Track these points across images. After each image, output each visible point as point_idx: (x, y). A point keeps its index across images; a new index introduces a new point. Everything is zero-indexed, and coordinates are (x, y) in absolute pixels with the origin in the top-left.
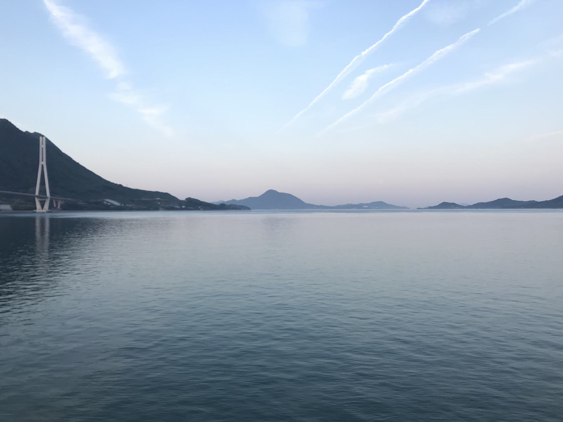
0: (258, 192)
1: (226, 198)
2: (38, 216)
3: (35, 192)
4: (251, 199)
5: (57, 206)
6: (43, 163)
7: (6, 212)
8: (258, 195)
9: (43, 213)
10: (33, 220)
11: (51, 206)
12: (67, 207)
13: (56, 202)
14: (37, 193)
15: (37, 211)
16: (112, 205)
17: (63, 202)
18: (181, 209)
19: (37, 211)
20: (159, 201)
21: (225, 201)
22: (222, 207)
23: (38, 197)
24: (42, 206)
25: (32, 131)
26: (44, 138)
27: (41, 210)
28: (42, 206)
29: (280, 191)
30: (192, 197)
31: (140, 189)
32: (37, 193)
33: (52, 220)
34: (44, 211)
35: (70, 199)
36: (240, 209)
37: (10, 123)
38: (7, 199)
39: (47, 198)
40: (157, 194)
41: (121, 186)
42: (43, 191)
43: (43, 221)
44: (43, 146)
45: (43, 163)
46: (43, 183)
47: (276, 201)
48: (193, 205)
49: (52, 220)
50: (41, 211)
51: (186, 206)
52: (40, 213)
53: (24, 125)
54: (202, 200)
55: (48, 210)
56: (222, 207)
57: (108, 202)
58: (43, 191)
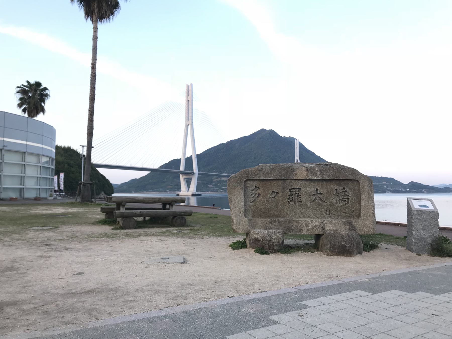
20: (385, 185)
25: (287, 136)
30: (415, 181)
37: (275, 132)
44: (297, 146)
53: (283, 133)
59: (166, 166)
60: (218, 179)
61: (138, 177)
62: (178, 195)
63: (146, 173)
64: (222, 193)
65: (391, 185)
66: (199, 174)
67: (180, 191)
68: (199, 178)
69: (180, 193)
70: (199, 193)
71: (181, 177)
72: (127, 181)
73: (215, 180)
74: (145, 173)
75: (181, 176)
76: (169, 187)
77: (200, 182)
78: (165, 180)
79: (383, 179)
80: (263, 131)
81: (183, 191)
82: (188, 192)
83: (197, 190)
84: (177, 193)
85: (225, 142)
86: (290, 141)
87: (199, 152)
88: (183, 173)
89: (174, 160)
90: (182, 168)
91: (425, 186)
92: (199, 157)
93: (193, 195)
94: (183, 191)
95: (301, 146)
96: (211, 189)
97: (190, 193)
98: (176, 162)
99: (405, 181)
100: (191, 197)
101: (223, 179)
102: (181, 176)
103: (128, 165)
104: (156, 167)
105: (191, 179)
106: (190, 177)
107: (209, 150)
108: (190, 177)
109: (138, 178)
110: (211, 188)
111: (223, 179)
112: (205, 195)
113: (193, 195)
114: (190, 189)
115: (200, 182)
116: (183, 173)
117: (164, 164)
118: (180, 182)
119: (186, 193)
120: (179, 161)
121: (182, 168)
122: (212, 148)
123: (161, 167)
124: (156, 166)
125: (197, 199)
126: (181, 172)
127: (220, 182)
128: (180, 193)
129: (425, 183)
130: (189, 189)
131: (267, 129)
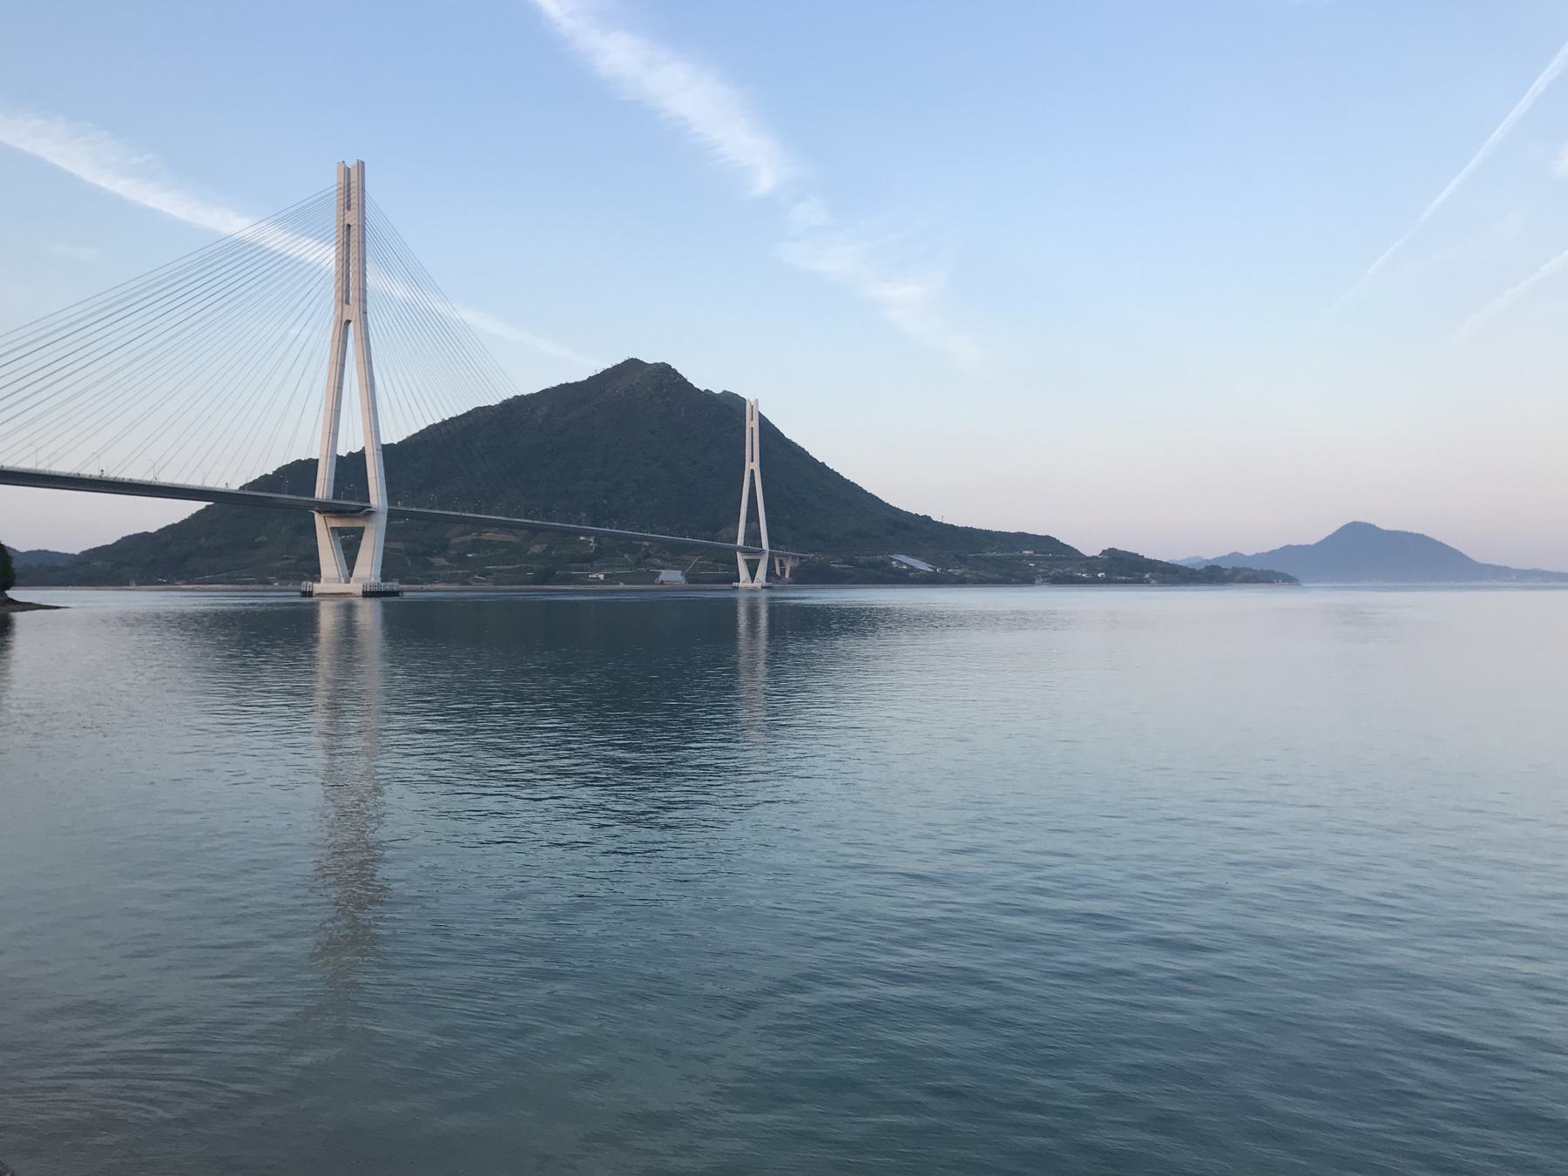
0: (1313, 529)
4: (1289, 551)
5: (783, 572)
6: (753, 465)
9: (754, 590)
10: (732, 605)
11: (770, 574)
13: (781, 564)
14: (740, 542)
15: (740, 585)
16: (912, 569)
17: (797, 563)
19: (740, 585)
21: (1249, 553)
25: (717, 391)
27: (750, 582)
29: (1386, 525)
31: (976, 527)
32: (740, 542)
37: (675, 372)
38: (675, 556)
39: (762, 552)
41: (927, 519)
42: (753, 536)
44: (752, 425)
45: (753, 465)
47: (1370, 554)
48: (1124, 568)
49: (772, 610)
53: (705, 376)
55: (765, 583)
57: (901, 563)
58: (753, 536)
59: (264, 482)
60: (468, 538)
62: (309, 594)
64: (486, 586)
66: (391, 515)
68: (391, 534)
69: (318, 588)
70: (394, 585)
75: (319, 520)
76: (278, 564)
77: (399, 545)
78: (263, 538)
79: (1022, 539)
80: (633, 365)
81: (327, 580)
82: (348, 582)
83: (385, 577)
84: (306, 585)
85: (495, 401)
87: (395, 432)
89: (299, 461)
90: (323, 488)
91: (1151, 561)
92: (391, 454)
93: (366, 594)
94: (327, 580)
95: (764, 423)
96: (442, 573)
97: (355, 587)
98: (302, 472)
100: (360, 602)
101: (489, 535)
102: (319, 520)
103: (91, 471)
105: (359, 533)
106: (358, 523)
107: (432, 429)
108: (358, 523)
109: (152, 530)
110: (443, 567)
111: (489, 535)
112: (411, 593)
113: (366, 594)
115: (399, 545)
116: (327, 509)
118: (316, 547)
119: (341, 587)
120: (312, 465)
121: (323, 488)
122: (444, 423)
125: (385, 606)
126: (319, 503)
127: (476, 546)
128: (318, 588)
129: (1149, 554)
131: (649, 359)
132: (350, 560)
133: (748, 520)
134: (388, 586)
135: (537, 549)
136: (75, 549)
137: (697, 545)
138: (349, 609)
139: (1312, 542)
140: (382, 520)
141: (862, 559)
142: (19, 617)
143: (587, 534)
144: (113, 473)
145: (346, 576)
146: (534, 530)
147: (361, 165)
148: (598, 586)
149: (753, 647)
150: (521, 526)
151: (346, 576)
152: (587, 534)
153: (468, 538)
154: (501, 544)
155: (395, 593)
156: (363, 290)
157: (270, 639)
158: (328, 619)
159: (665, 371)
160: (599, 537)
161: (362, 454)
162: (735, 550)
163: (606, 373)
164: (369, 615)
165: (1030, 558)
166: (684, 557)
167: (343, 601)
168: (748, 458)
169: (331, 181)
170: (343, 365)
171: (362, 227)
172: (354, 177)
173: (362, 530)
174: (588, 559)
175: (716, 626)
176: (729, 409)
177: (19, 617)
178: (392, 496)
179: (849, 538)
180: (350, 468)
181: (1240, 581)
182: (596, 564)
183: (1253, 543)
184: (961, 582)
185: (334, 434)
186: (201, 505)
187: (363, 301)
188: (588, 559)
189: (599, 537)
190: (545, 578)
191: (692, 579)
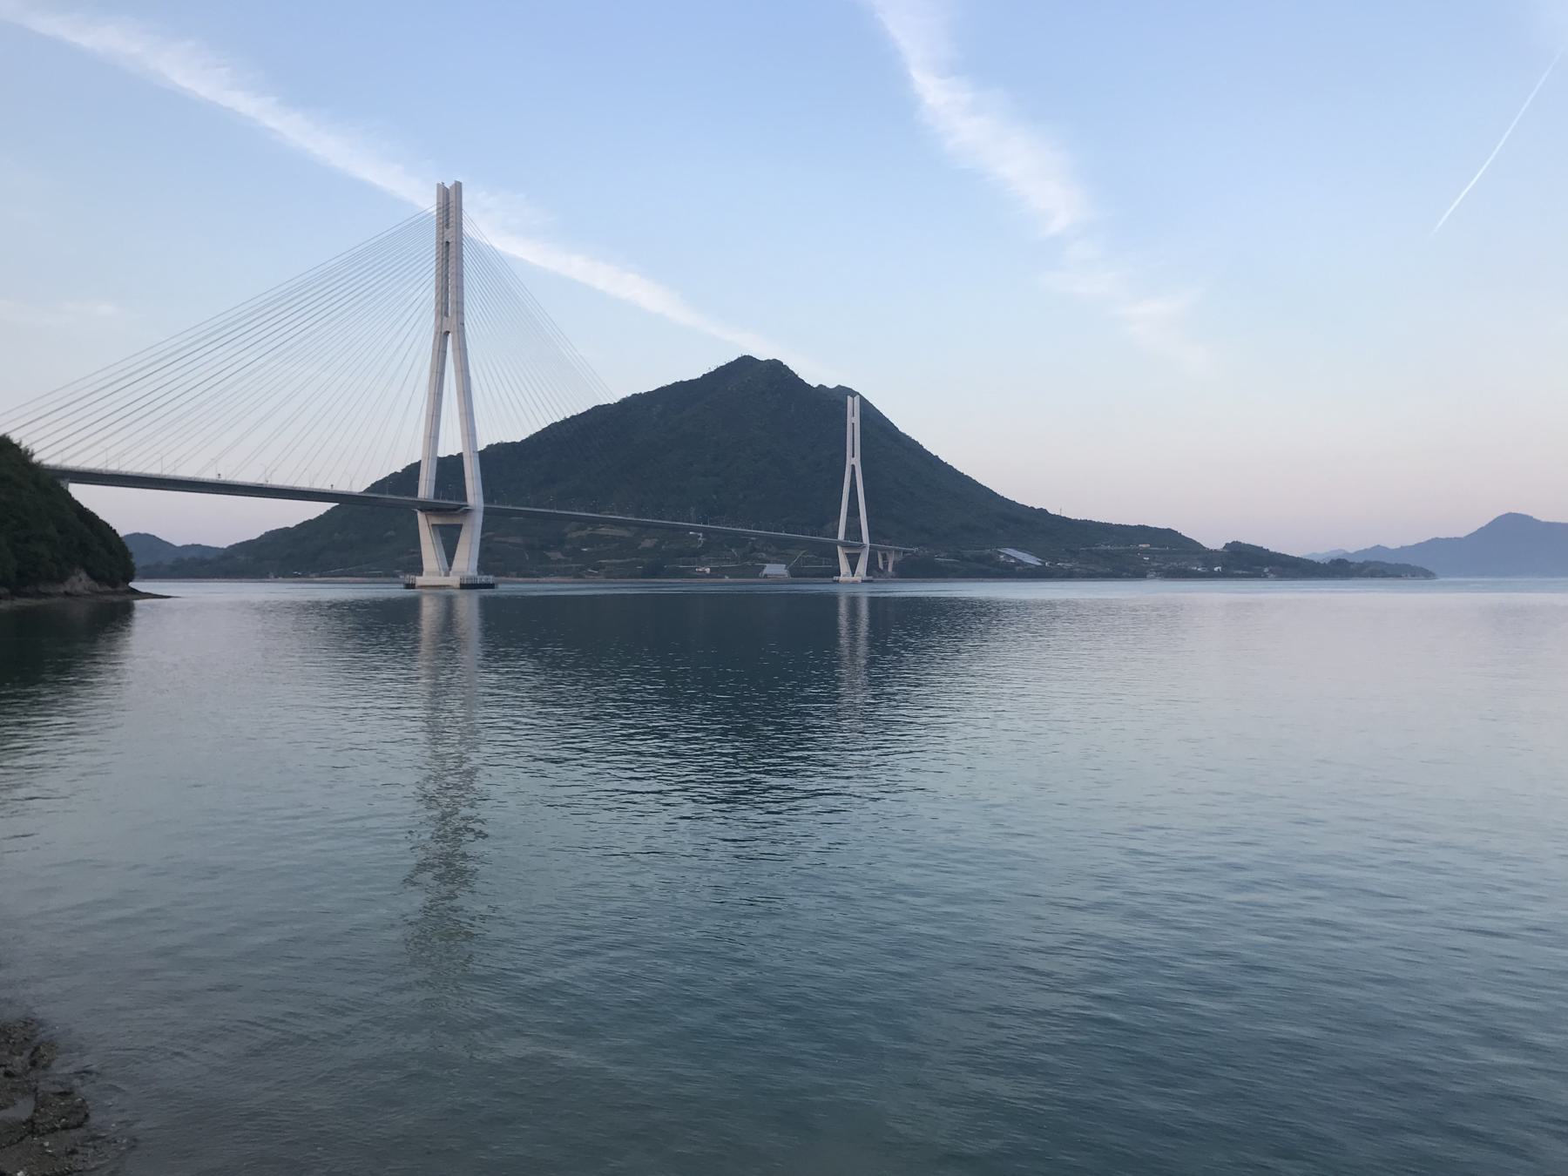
1: (1351, 544)
2: (843, 592)
3: (836, 534)
5: (886, 566)
6: (854, 460)
7: (777, 580)
8: (1463, 532)
9: (855, 583)
10: (833, 600)
11: (872, 568)
12: (908, 571)
13: (885, 558)
14: (841, 536)
18: (1210, 575)
21: (1351, 551)
22: (1339, 569)
23: (845, 546)
24: (853, 568)
26: (857, 399)
27: (852, 579)
28: (853, 568)
30: (1245, 540)
31: (1096, 520)
32: (841, 536)
33: (873, 602)
34: (857, 578)
35: (915, 550)
36: (1399, 576)
38: (780, 551)
39: (862, 546)
40: (1143, 532)
41: (1043, 512)
42: (853, 530)
43: (853, 602)
44: (853, 419)
45: (854, 460)
46: (853, 511)
48: (1245, 562)
49: (873, 602)
50: (851, 579)
51: (1224, 566)
52: (846, 583)
53: (814, 372)
54: (1273, 547)
56: (1339, 569)
57: (1009, 556)
58: (853, 530)
60: (583, 533)
61: (292, 523)
62: (411, 586)
63: (329, 506)
64: (598, 579)
65: (1162, 553)
66: (486, 512)
67: (420, 572)
69: (420, 580)
70: (491, 579)
71: (423, 522)
72: (255, 537)
73: (574, 535)
74: (318, 509)
75: (421, 517)
78: (391, 533)
80: (746, 362)
81: (432, 573)
82: (447, 575)
84: (409, 578)
85: (613, 399)
86: (833, 401)
88: (428, 508)
90: (426, 489)
93: (463, 586)
94: (432, 573)
97: (454, 580)
98: (413, 471)
99: (1214, 540)
101: (604, 531)
102: (421, 517)
103: (209, 475)
104: (359, 486)
108: (456, 521)
110: (559, 561)
111: (604, 531)
112: (510, 587)
113: (463, 586)
114: (457, 564)
116: (428, 508)
117: (386, 474)
121: (425, 490)
122: (566, 420)
123: (377, 487)
124: (358, 485)
128: (420, 580)
130: (450, 564)
132: (450, 555)
133: (849, 514)
134: (484, 579)
135: (648, 543)
136: (224, 544)
137: (797, 540)
138: (449, 602)
139: (1462, 535)
140: (478, 519)
141: (968, 553)
142: (138, 603)
143: (697, 530)
144: (229, 476)
145: (445, 568)
146: (648, 526)
147: (458, 186)
148: (706, 581)
149: (854, 639)
150: (630, 523)
151: (445, 568)
152: (697, 530)
153: (583, 533)
154: (614, 539)
155: (491, 586)
156: (460, 303)
157: (384, 628)
158: (429, 610)
159: (776, 367)
160: (706, 532)
161: (460, 455)
162: (835, 546)
163: (720, 370)
164: (468, 608)
165: (1146, 552)
166: (790, 551)
167: (442, 592)
168: (849, 453)
169: (429, 204)
170: (442, 373)
171: (460, 244)
172: (452, 198)
173: (459, 527)
174: (696, 554)
175: (814, 623)
176: (830, 404)
177: (138, 603)
178: (489, 495)
179: (955, 529)
180: (450, 469)
181: (1366, 576)
182: (704, 558)
183: (1396, 536)
184: (1069, 575)
185: (433, 436)
186: (329, 506)
187: (460, 313)
188: (696, 554)
189: (706, 532)
190: (653, 572)
191: (796, 573)
